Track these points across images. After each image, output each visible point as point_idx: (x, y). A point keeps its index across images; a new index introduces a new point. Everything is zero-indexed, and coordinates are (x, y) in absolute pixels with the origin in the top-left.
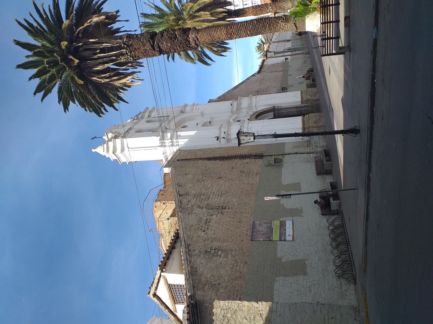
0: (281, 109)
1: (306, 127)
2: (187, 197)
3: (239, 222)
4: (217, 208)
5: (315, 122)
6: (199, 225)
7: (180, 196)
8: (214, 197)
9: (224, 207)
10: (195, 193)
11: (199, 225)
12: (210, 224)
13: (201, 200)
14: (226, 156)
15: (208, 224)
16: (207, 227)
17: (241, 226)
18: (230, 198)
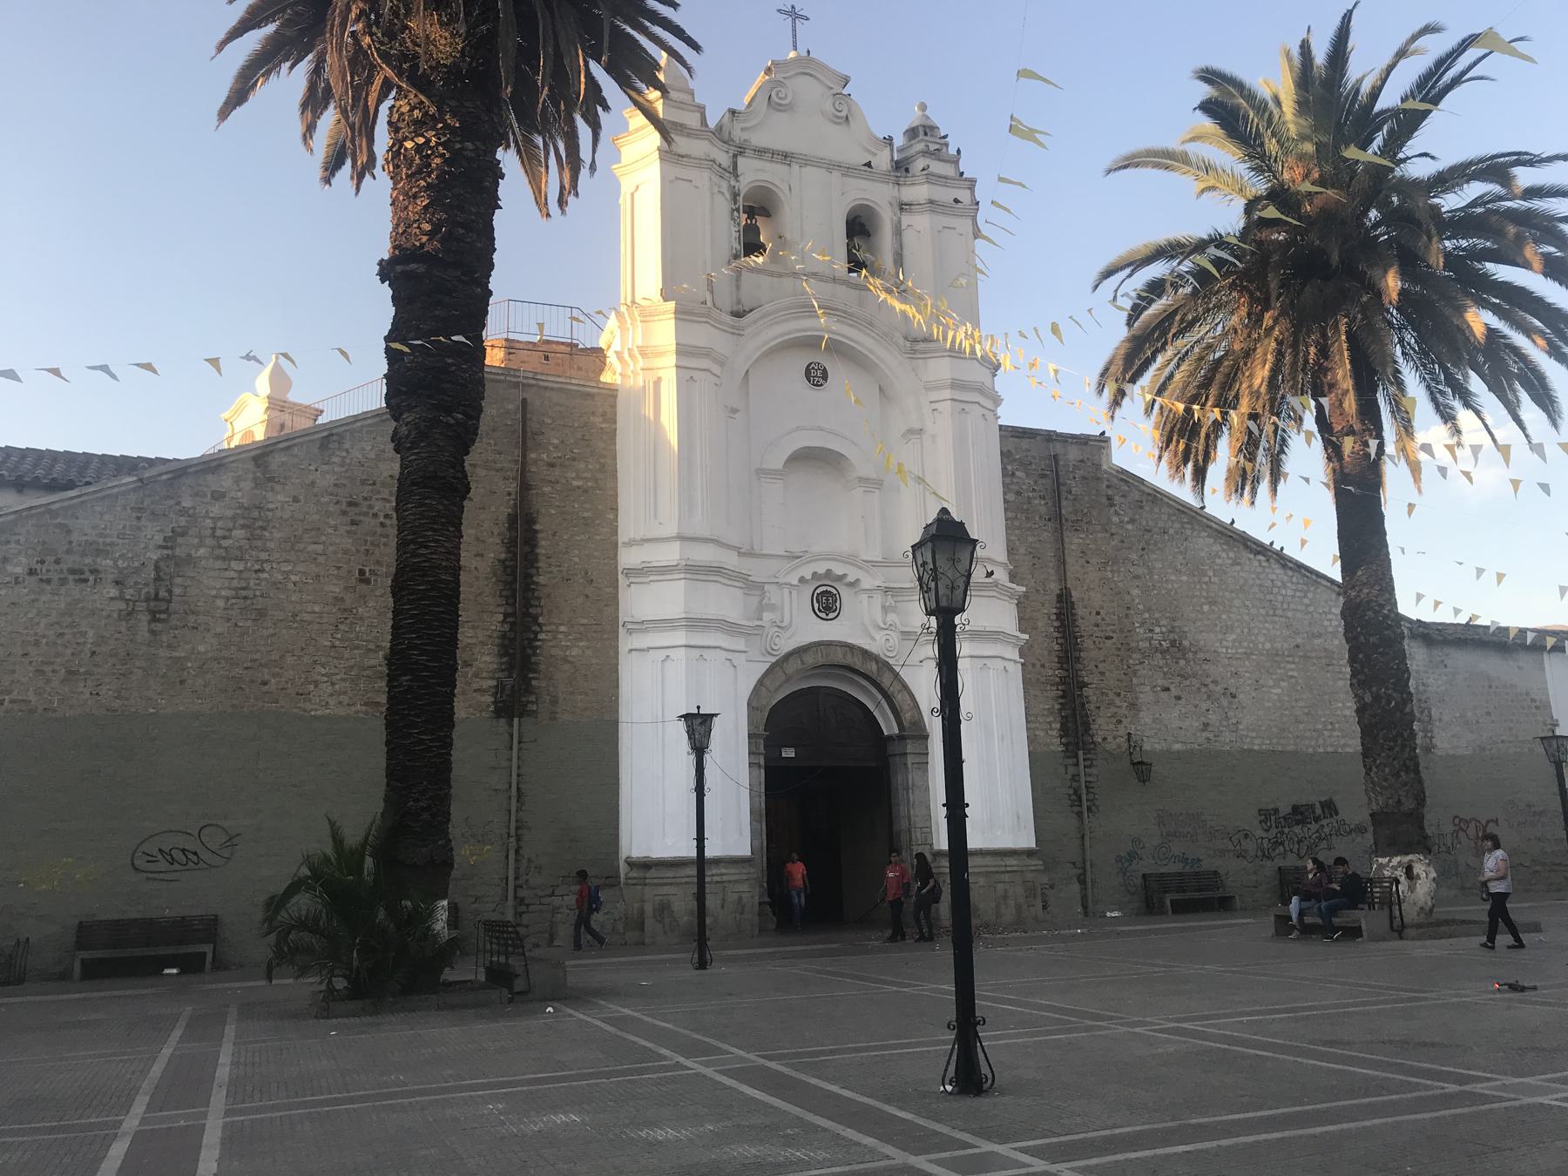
1: (653, 873)
2: (247, 485)
3: (69, 672)
4: (163, 594)
5: (663, 909)
6: (68, 552)
7: (255, 459)
8: (232, 574)
9: (163, 616)
10: (271, 506)
11: (68, 552)
12: (71, 585)
13: (219, 533)
14: (541, 579)
15: (71, 577)
16: (55, 577)
17: (48, 681)
18: (219, 630)
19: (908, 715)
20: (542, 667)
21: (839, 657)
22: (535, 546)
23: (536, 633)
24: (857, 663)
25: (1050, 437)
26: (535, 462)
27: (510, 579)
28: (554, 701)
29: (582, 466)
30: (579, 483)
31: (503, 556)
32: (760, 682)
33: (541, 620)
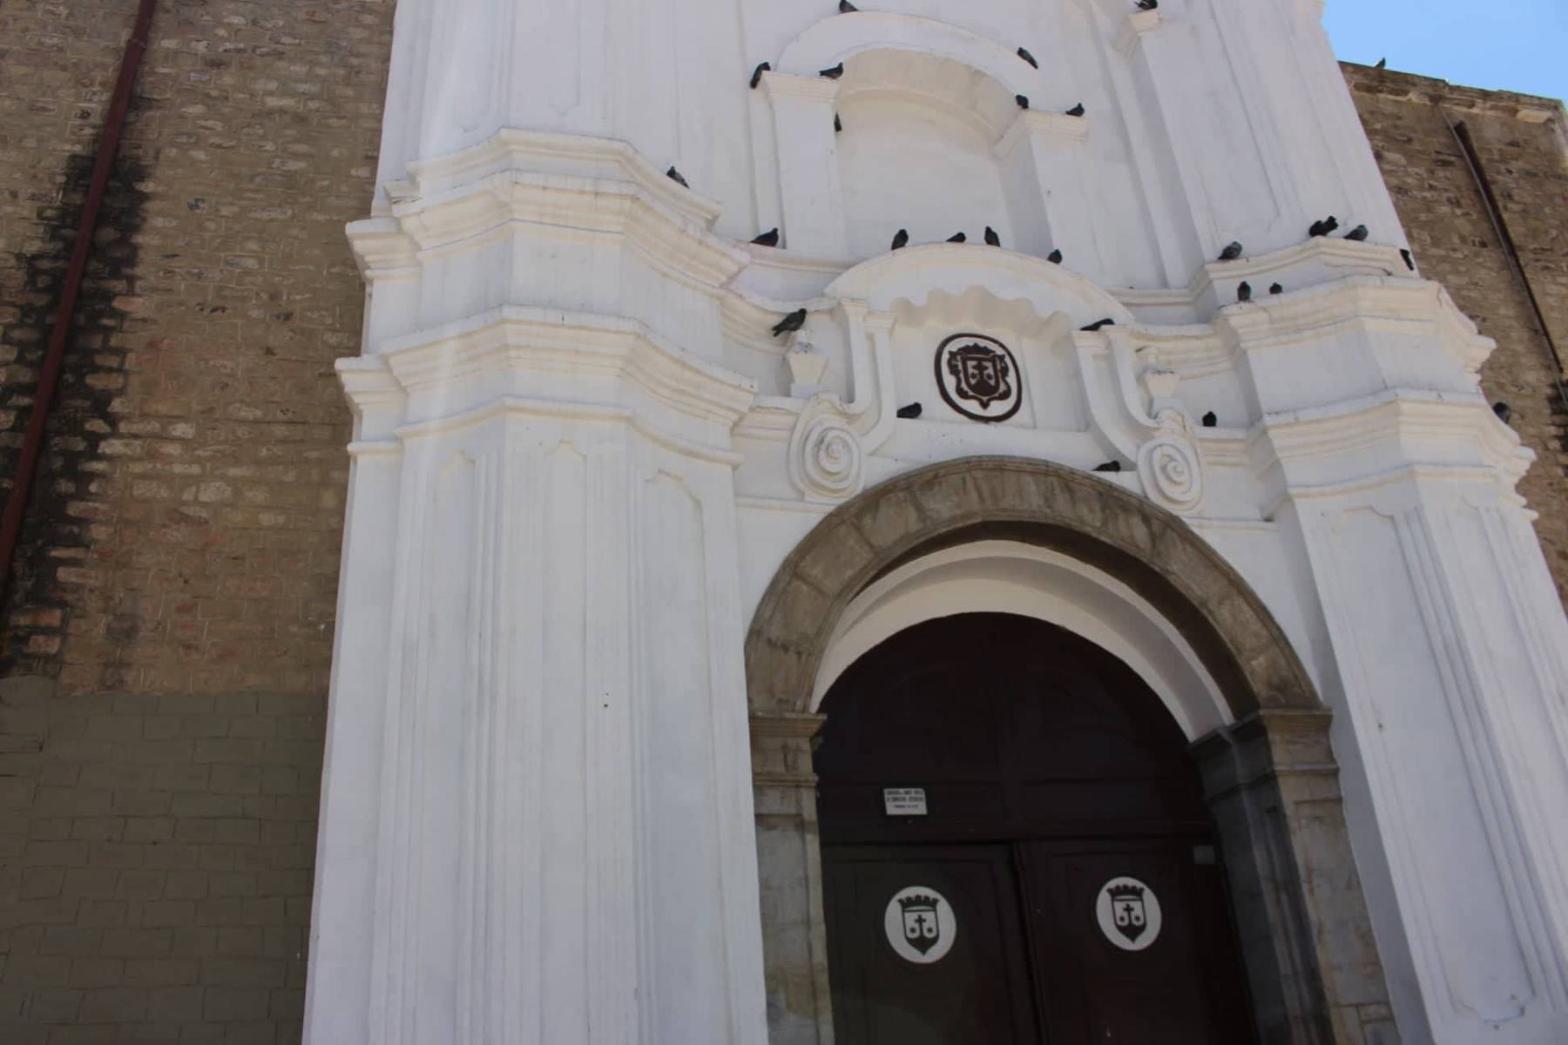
0: (1275, 812)
14: (137, 306)
19: (1256, 667)
20: (99, 532)
21: (1030, 502)
22: (136, 229)
23: (95, 439)
24: (1089, 520)
25: (1437, 91)
26: (177, 53)
27: (42, 301)
28: (125, 631)
29: (299, 69)
30: (286, 102)
31: (33, 247)
32: (793, 568)
33: (117, 405)
